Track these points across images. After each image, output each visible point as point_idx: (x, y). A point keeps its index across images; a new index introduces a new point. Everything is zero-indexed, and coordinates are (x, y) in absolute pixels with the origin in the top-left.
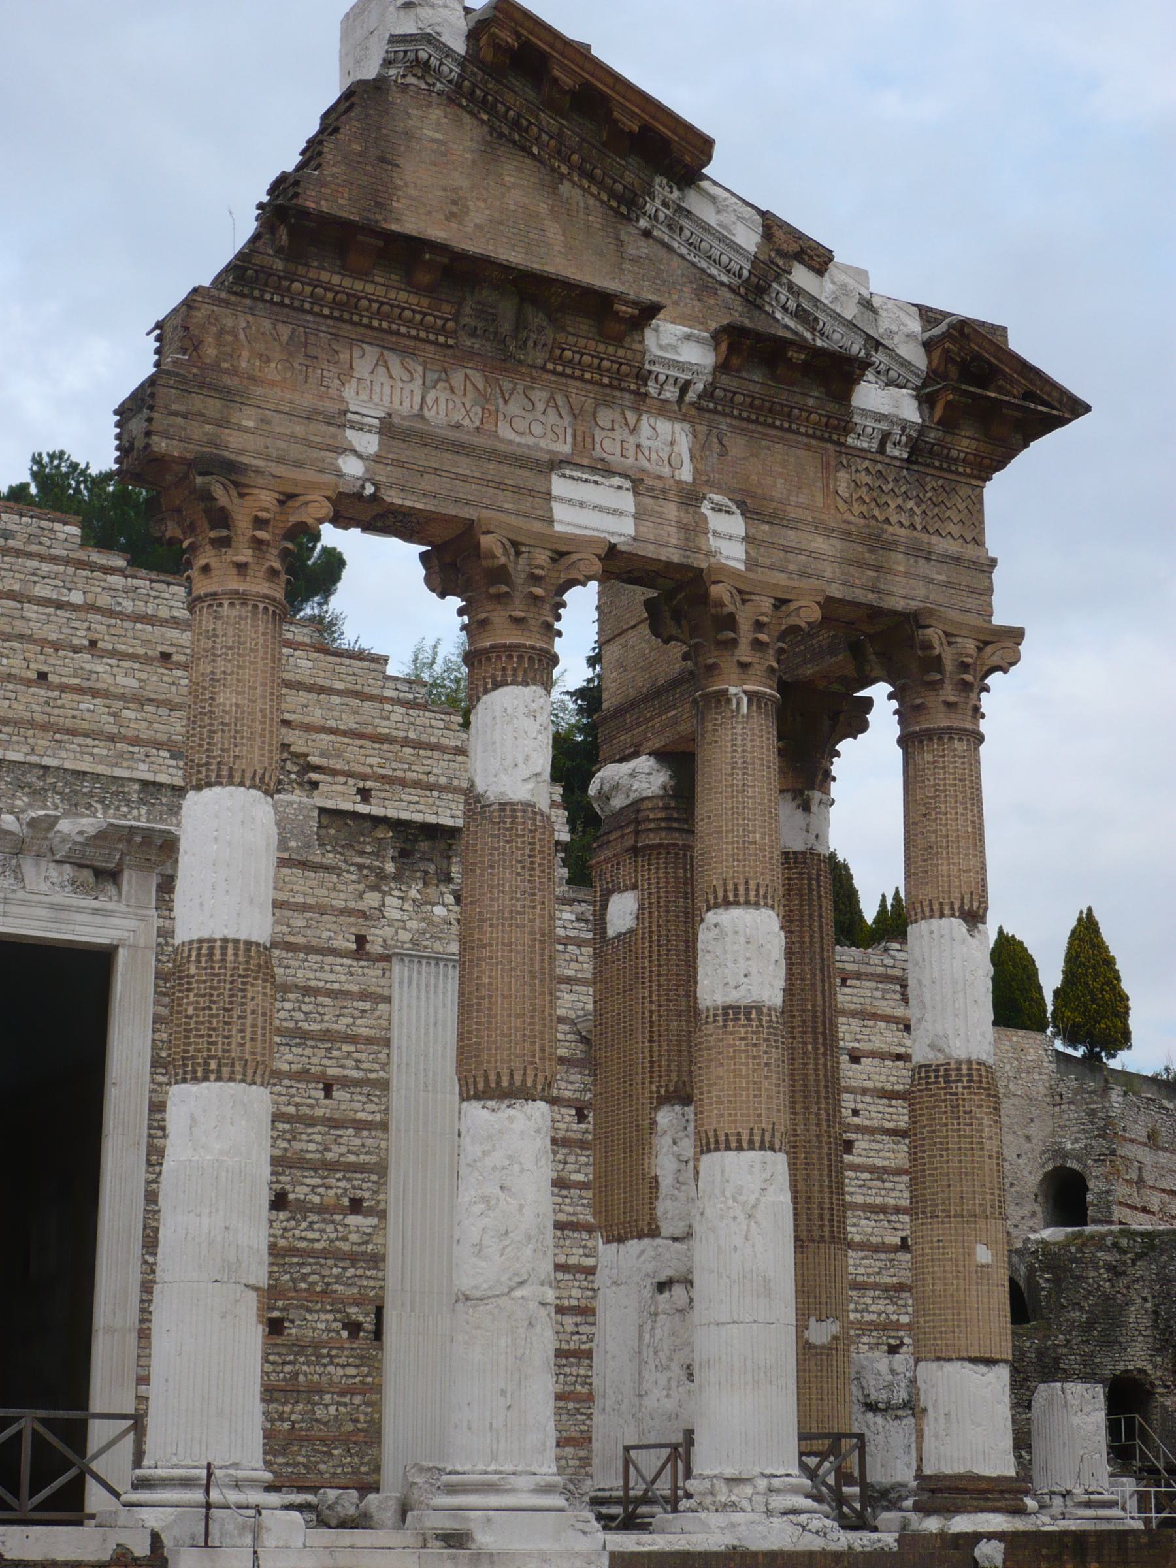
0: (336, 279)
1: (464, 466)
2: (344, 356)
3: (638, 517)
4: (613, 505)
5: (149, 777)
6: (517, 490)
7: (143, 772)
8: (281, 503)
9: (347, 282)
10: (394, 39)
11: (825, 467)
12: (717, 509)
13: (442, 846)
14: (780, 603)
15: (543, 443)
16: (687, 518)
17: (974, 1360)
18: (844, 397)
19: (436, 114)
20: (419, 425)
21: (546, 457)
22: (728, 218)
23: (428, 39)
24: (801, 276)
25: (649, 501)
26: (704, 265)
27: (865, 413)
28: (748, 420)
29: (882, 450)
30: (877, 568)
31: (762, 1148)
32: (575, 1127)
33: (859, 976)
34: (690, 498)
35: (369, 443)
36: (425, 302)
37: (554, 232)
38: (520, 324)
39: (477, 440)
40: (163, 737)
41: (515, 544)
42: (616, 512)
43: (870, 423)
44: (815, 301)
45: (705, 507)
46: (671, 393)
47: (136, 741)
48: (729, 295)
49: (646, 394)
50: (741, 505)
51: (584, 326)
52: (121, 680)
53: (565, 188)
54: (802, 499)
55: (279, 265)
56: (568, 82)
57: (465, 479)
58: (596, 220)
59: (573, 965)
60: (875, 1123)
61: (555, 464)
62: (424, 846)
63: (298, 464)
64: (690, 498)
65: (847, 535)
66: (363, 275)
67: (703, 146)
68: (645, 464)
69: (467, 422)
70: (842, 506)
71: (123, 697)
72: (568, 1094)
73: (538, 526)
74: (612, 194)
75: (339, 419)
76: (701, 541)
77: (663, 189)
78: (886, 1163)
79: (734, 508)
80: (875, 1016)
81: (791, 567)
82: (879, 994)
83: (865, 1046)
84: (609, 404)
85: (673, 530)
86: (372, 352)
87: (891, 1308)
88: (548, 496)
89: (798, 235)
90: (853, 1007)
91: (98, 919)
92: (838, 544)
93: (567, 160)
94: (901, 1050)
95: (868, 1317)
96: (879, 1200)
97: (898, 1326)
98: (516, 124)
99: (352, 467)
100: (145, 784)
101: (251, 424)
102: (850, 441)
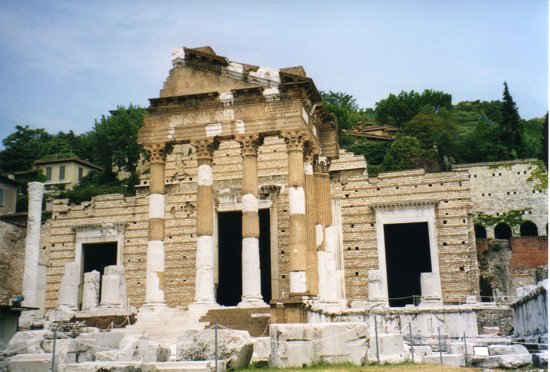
0: (163, 107)
1: (189, 130)
2: (169, 118)
3: (222, 129)
4: (217, 129)
5: (273, 175)
6: (199, 131)
7: (272, 174)
8: (158, 146)
9: (165, 107)
10: (173, 61)
11: (262, 107)
12: (239, 123)
13: (338, 174)
14: (251, 137)
15: (205, 122)
16: (232, 127)
17: (294, 271)
18: (261, 94)
19: (184, 70)
20: (182, 126)
21: (204, 124)
22: (235, 69)
23: (179, 58)
24: (252, 73)
25: (224, 126)
26: (235, 78)
27: (267, 95)
28: (245, 104)
29: (275, 101)
30: (273, 124)
31: (248, 237)
32: (371, 228)
33: (446, 182)
34: (233, 123)
35: (172, 132)
36: (179, 105)
37: (206, 83)
38: (196, 103)
39: (193, 125)
40: (275, 167)
41: (198, 142)
42: (218, 130)
43: (269, 97)
44: (256, 77)
45: (236, 124)
46: (228, 104)
47: (270, 169)
48: (241, 82)
49: (224, 106)
50: (243, 120)
51: (207, 99)
52: (267, 158)
53: (208, 74)
54: (258, 115)
55: (154, 108)
56: (199, 57)
57: (190, 132)
58: (214, 77)
59: (369, 193)
60: (453, 216)
61: (206, 125)
62: (335, 175)
63: (161, 139)
64: (233, 123)
65: (266, 119)
66: (167, 105)
67: (223, 58)
68: (224, 119)
69: (191, 122)
70: (266, 114)
71: (267, 161)
72: (369, 221)
73: (204, 137)
74: (216, 72)
75: (167, 130)
76: (236, 130)
77: (222, 68)
78: (456, 225)
79: (242, 121)
80: (451, 191)
81: (254, 129)
82: (452, 185)
83: (449, 198)
84: (217, 110)
85: (229, 130)
86: (174, 116)
87: (460, 258)
88: (205, 131)
89: (250, 66)
90: (444, 190)
91: (266, 204)
92: (264, 122)
93: (206, 69)
94: (460, 197)
95: (453, 261)
96: (455, 234)
97: (462, 262)
98: (196, 66)
99: (170, 137)
100: (273, 176)
101: (153, 135)
102: (267, 101)
